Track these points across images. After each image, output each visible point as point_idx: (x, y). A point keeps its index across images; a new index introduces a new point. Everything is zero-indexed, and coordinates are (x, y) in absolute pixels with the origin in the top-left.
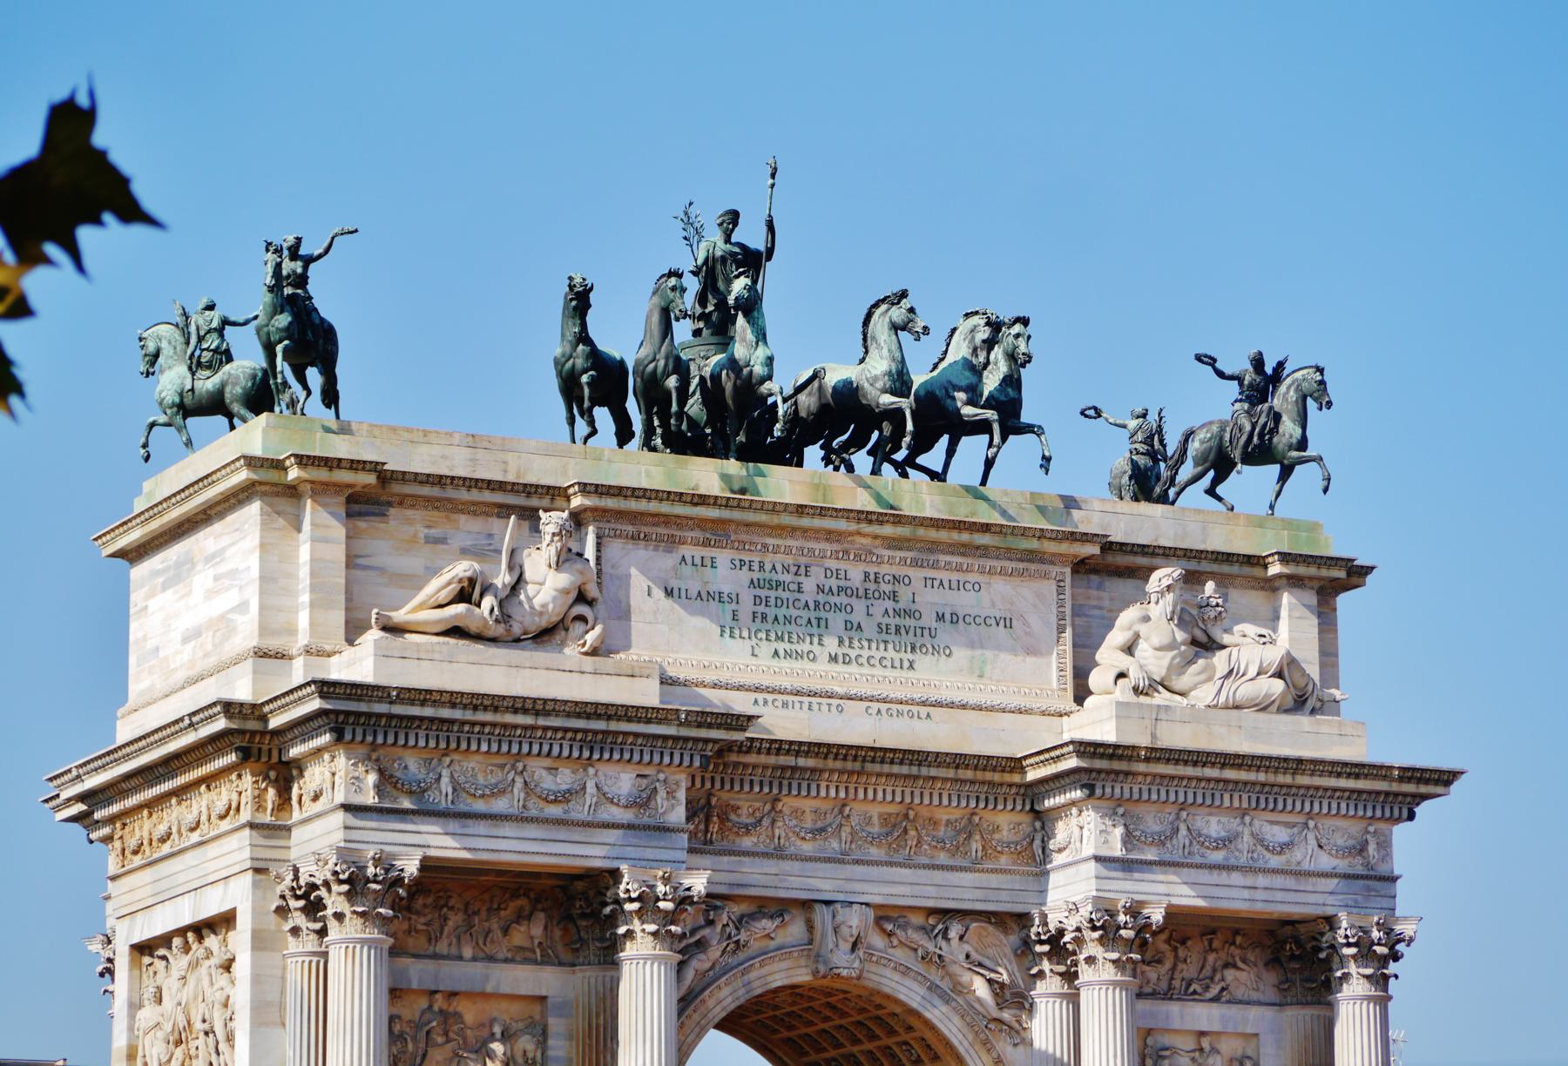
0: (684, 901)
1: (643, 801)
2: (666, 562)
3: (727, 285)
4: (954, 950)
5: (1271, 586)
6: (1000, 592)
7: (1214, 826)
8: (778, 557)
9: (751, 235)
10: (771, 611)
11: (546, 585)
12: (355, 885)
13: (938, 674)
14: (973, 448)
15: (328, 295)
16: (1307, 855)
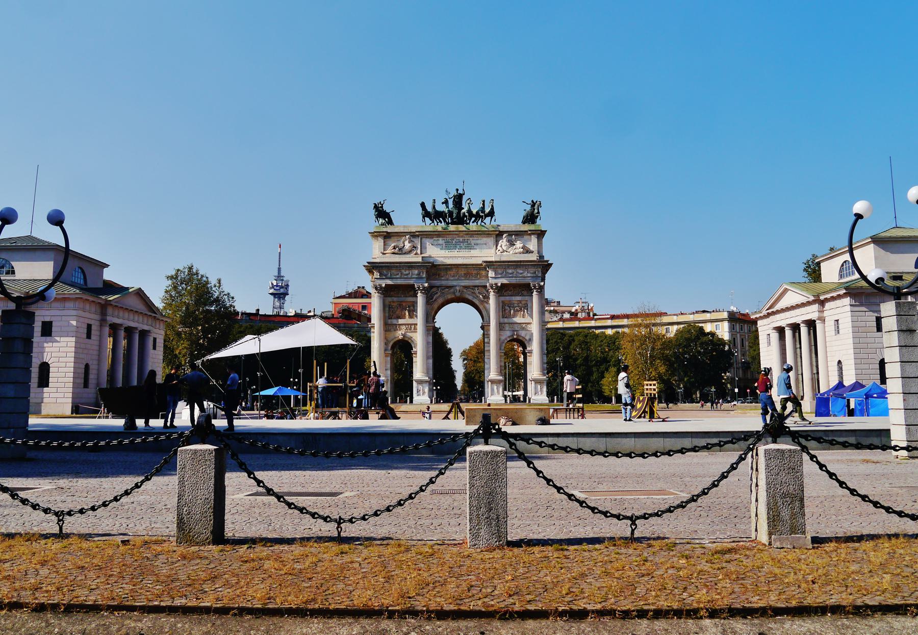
0: (424, 288)
1: (419, 274)
2: (432, 240)
3: (458, 199)
4: (477, 291)
5: (530, 235)
6: (485, 240)
7: (510, 271)
8: (449, 239)
9: (461, 192)
10: (448, 246)
11: (408, 245)
12: (376, 288)
13: (473, 252)
14: (488, 219)
15: (386, 208)
16: (525, 274)
